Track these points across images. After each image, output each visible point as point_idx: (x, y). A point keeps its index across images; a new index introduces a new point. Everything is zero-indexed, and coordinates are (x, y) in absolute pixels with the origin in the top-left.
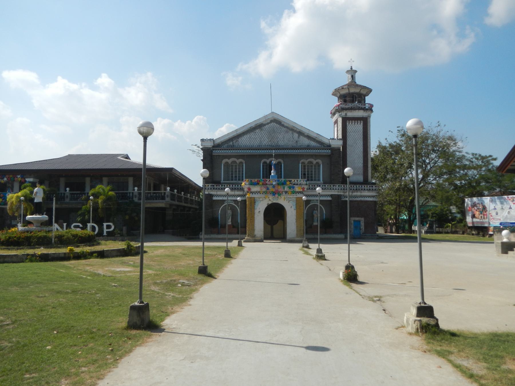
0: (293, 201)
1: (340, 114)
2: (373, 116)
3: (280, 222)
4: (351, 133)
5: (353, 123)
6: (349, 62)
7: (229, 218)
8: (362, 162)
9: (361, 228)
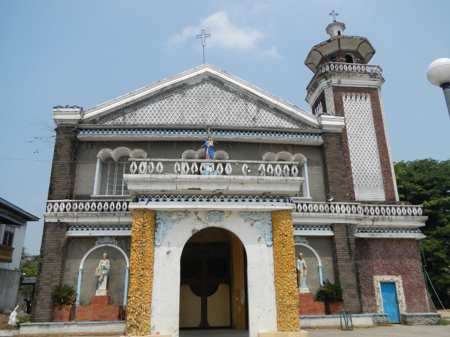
0: (263, 223)
1: (329, 81)
2: (383, 86)
3: (222, 289)
4: (351, 114)
5: (353, 98)
6: (330, 14)
7: (102, 280)
8: (379, 165)
9: (399, 299)
